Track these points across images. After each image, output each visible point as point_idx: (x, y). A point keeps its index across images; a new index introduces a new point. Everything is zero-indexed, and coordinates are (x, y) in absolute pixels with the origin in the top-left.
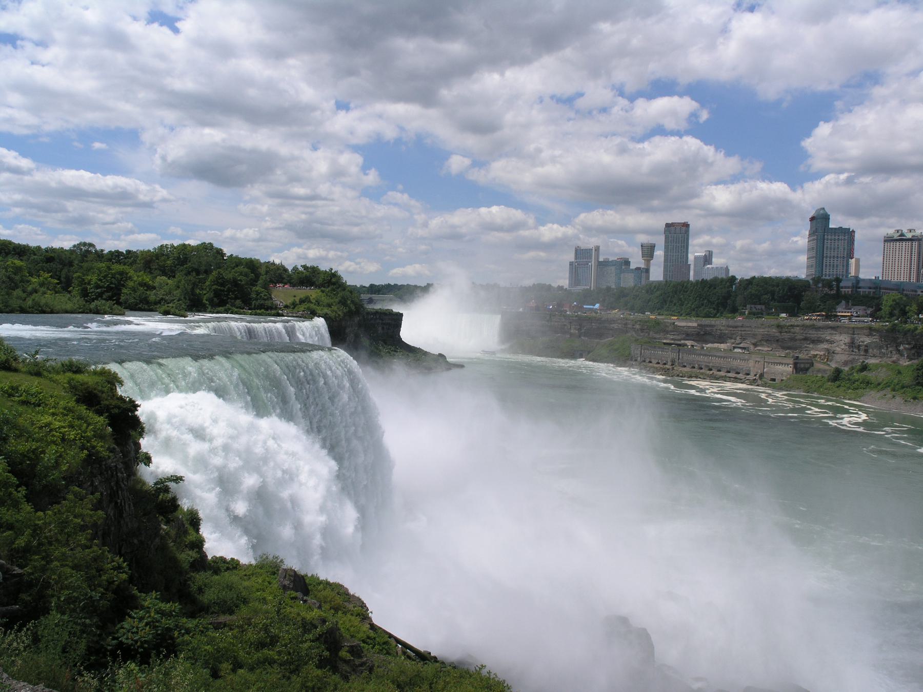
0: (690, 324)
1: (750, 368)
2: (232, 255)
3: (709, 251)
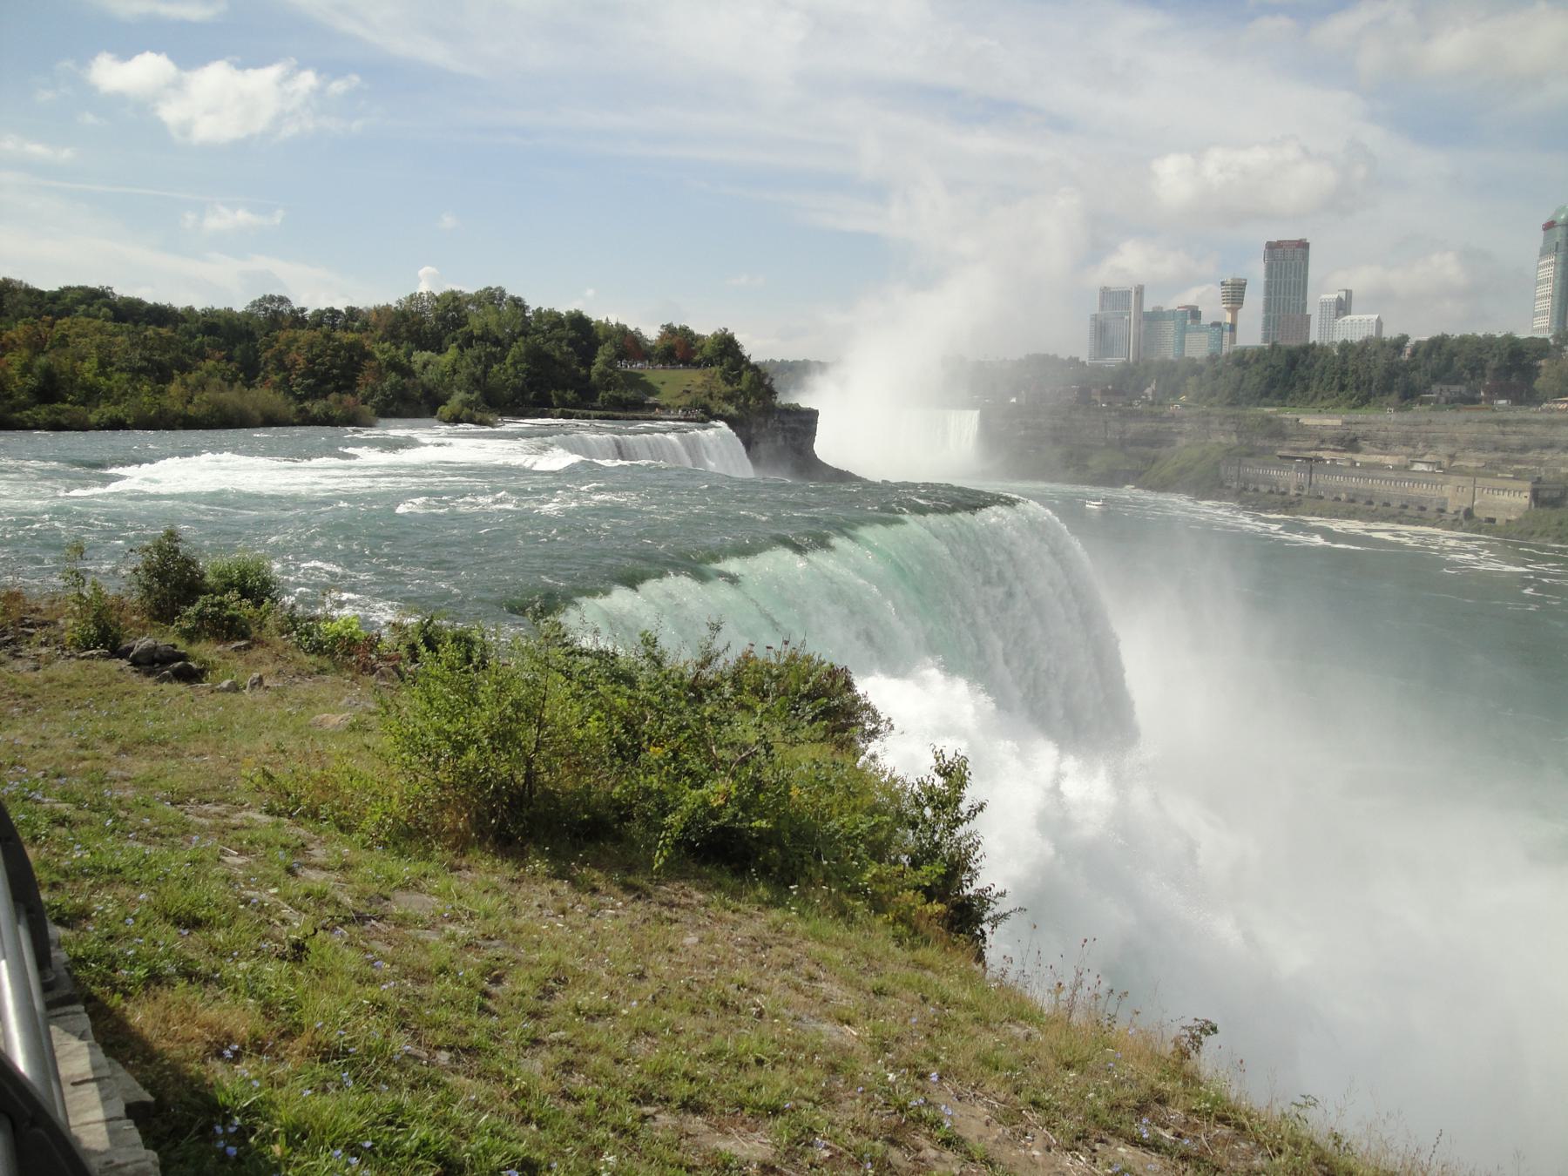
0: (1328, 422)
1: (1446, 499)
2: (540, 309)
3: (1347, 291)
